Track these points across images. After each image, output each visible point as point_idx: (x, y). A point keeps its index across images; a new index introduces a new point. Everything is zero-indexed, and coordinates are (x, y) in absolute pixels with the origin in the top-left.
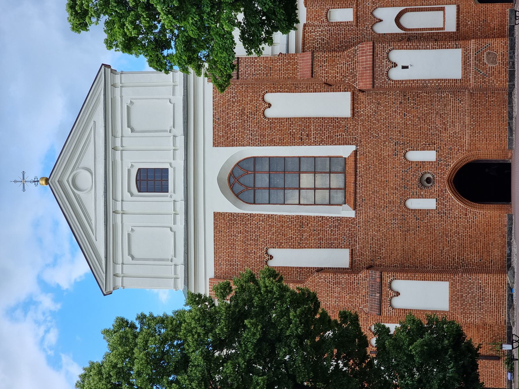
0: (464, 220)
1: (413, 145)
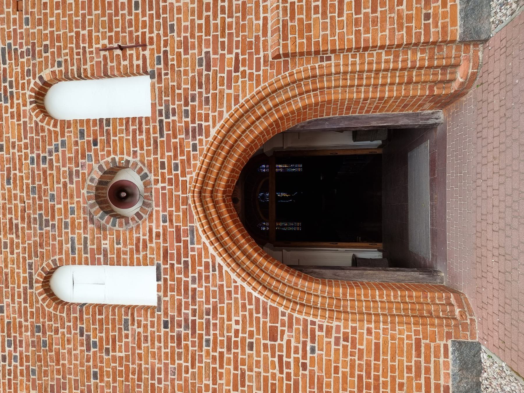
0: (266, 358)
1: (66, 54)
